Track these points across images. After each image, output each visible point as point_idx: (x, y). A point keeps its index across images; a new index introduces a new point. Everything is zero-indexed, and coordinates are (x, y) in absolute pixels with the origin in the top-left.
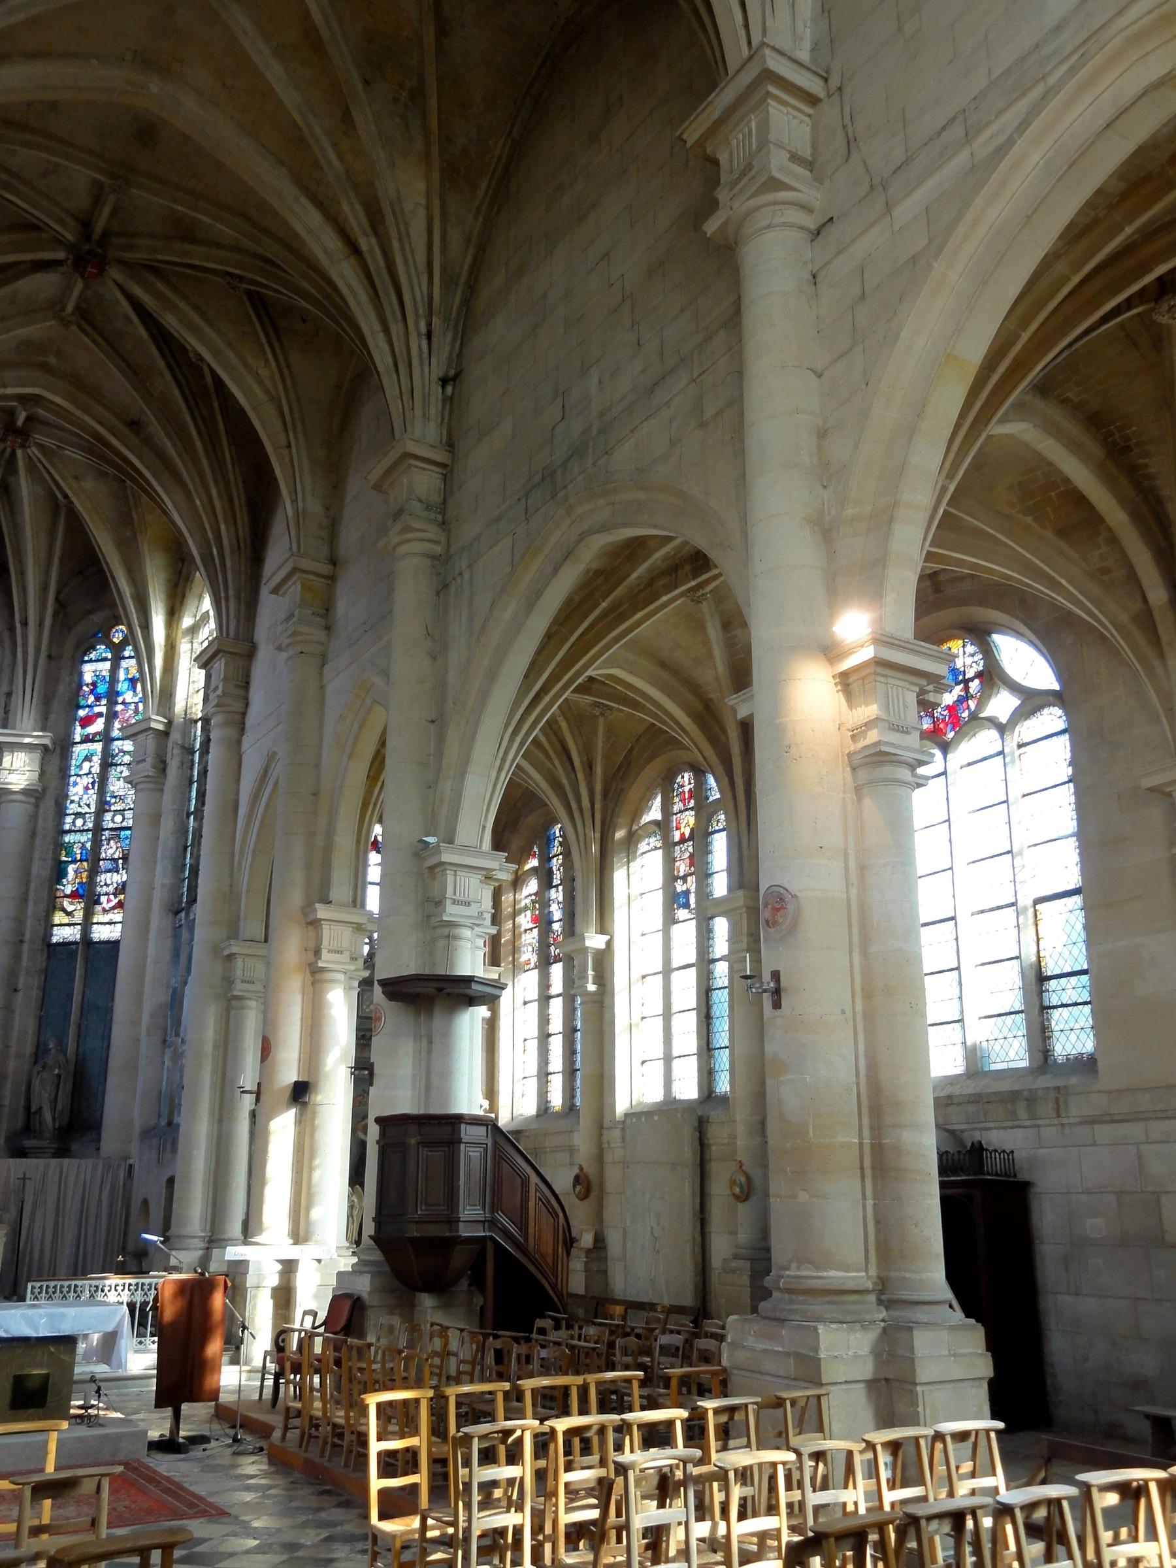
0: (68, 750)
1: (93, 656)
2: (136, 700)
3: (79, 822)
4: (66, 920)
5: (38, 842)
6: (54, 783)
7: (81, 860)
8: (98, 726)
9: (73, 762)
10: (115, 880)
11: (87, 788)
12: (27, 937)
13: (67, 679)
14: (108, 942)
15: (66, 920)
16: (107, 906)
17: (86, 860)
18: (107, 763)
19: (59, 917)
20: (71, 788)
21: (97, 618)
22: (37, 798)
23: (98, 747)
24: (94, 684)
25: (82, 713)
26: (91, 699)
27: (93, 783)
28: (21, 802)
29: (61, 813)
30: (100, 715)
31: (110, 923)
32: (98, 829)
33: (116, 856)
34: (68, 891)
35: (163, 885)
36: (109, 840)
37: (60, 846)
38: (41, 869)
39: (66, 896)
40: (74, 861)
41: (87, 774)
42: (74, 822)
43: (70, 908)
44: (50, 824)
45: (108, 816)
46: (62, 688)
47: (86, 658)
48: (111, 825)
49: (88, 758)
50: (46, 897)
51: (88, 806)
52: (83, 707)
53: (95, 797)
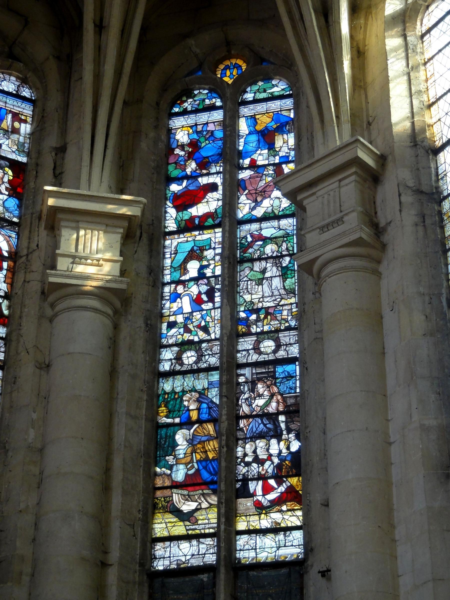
0: (159, 243)
1: (188, 105)
2: (277, 160)
3: (189, 358)
4: (180, 529)
5: (123, 384)
6: (142, 291)
7: (200, 421)
8: (211, 203)
9: (168, 262)
10: (274, 450)
11: (197, 301)
12: (115, 555)
13: (152, 134)
14: (277, 565)
15: (180, 529)
16: (266, 500)
17: (214, 421)
18: (235, 257)
19: (162, 525)
20: (168, 305)
21: (197, 45)
22: (116, 312)
23: (216, 236)
24: (194, 145)
25: (175, 188)
26: (192, 166)
27: (210, 294)
28: (96, 310)
29: (156, 345)
30: (213, 187)
31: (276, 530)
32: (230, 366)
33: (273, 407)
34: (180, 474)
35: (424, 429)
36: (253, 384)
37: (154, 398)
38: (128, 434)
39: (176, 486)
40: (187, 423)
41: (195, 280)
42: (178, 359)
43: (188, 507)
44: (140, 358)
45: (246, 344)
46: (144, 145)
47: (176, 110)
48: (254, 357)
49: (196, 254)
50: (141, 485)
51: (205, 329)
52: (179, 180)
53: (217, 314)
